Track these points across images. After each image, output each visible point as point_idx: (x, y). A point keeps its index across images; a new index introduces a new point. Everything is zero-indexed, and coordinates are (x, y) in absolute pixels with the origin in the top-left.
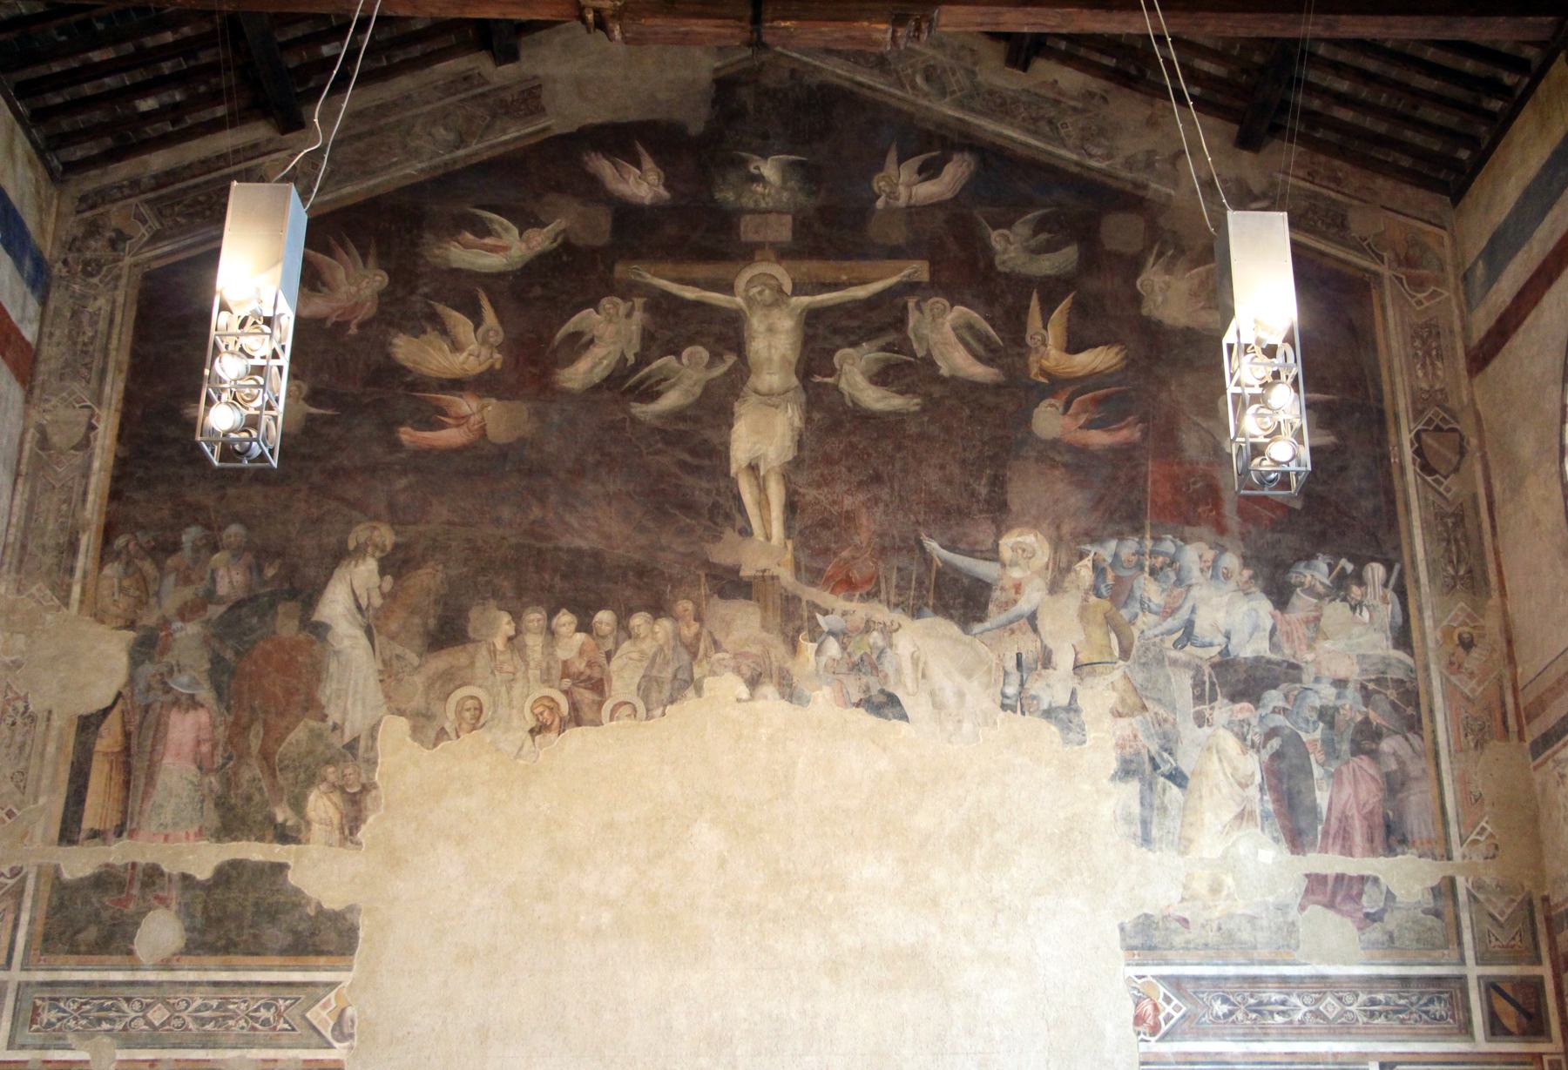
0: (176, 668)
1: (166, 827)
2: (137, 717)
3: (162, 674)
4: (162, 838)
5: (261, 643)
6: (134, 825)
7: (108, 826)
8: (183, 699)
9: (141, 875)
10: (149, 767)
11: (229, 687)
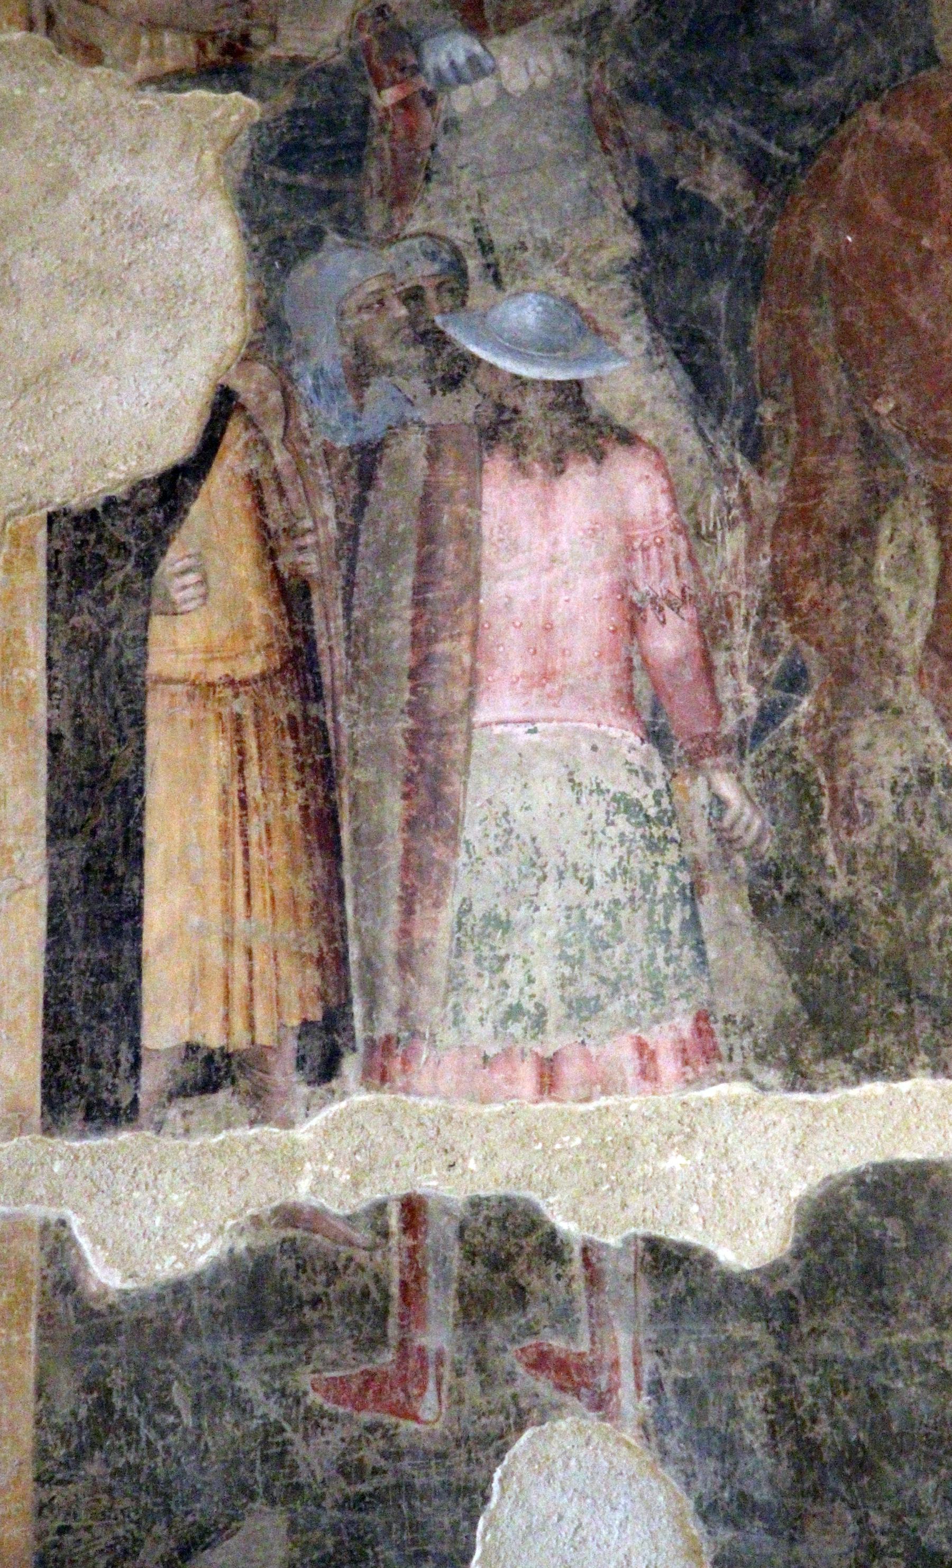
0: (473, 264)
1: (539, 1022)
2: (327, 508)
3: (414, 296)
4: (527, 1074)
5: (872, 115)
6: (387, 1023)
7: (264, 1036)
8: (532, 407)
9: (455, 1253)
10: (415, 739)
11: (739, 343)
